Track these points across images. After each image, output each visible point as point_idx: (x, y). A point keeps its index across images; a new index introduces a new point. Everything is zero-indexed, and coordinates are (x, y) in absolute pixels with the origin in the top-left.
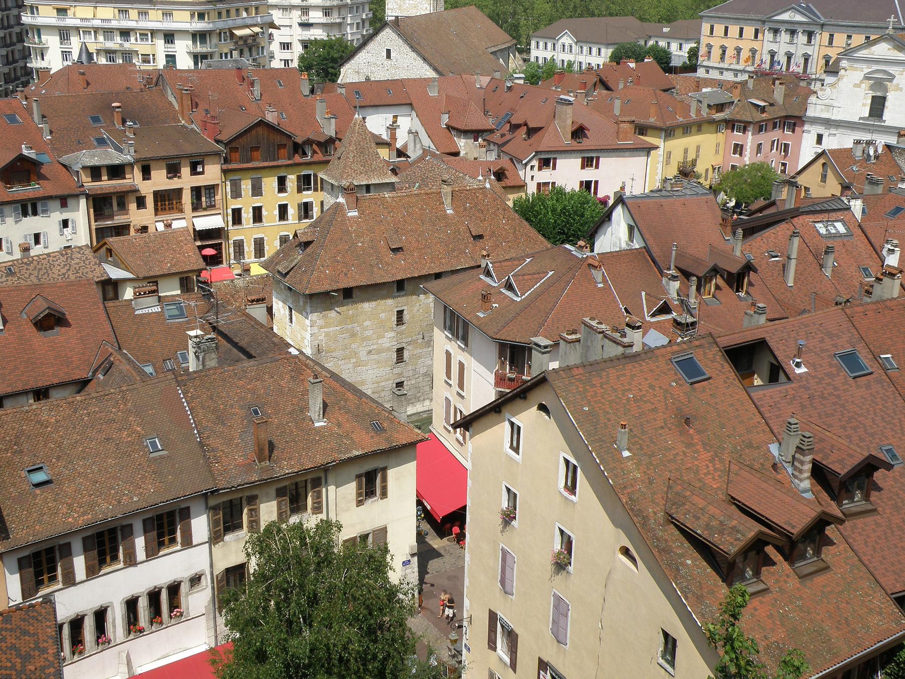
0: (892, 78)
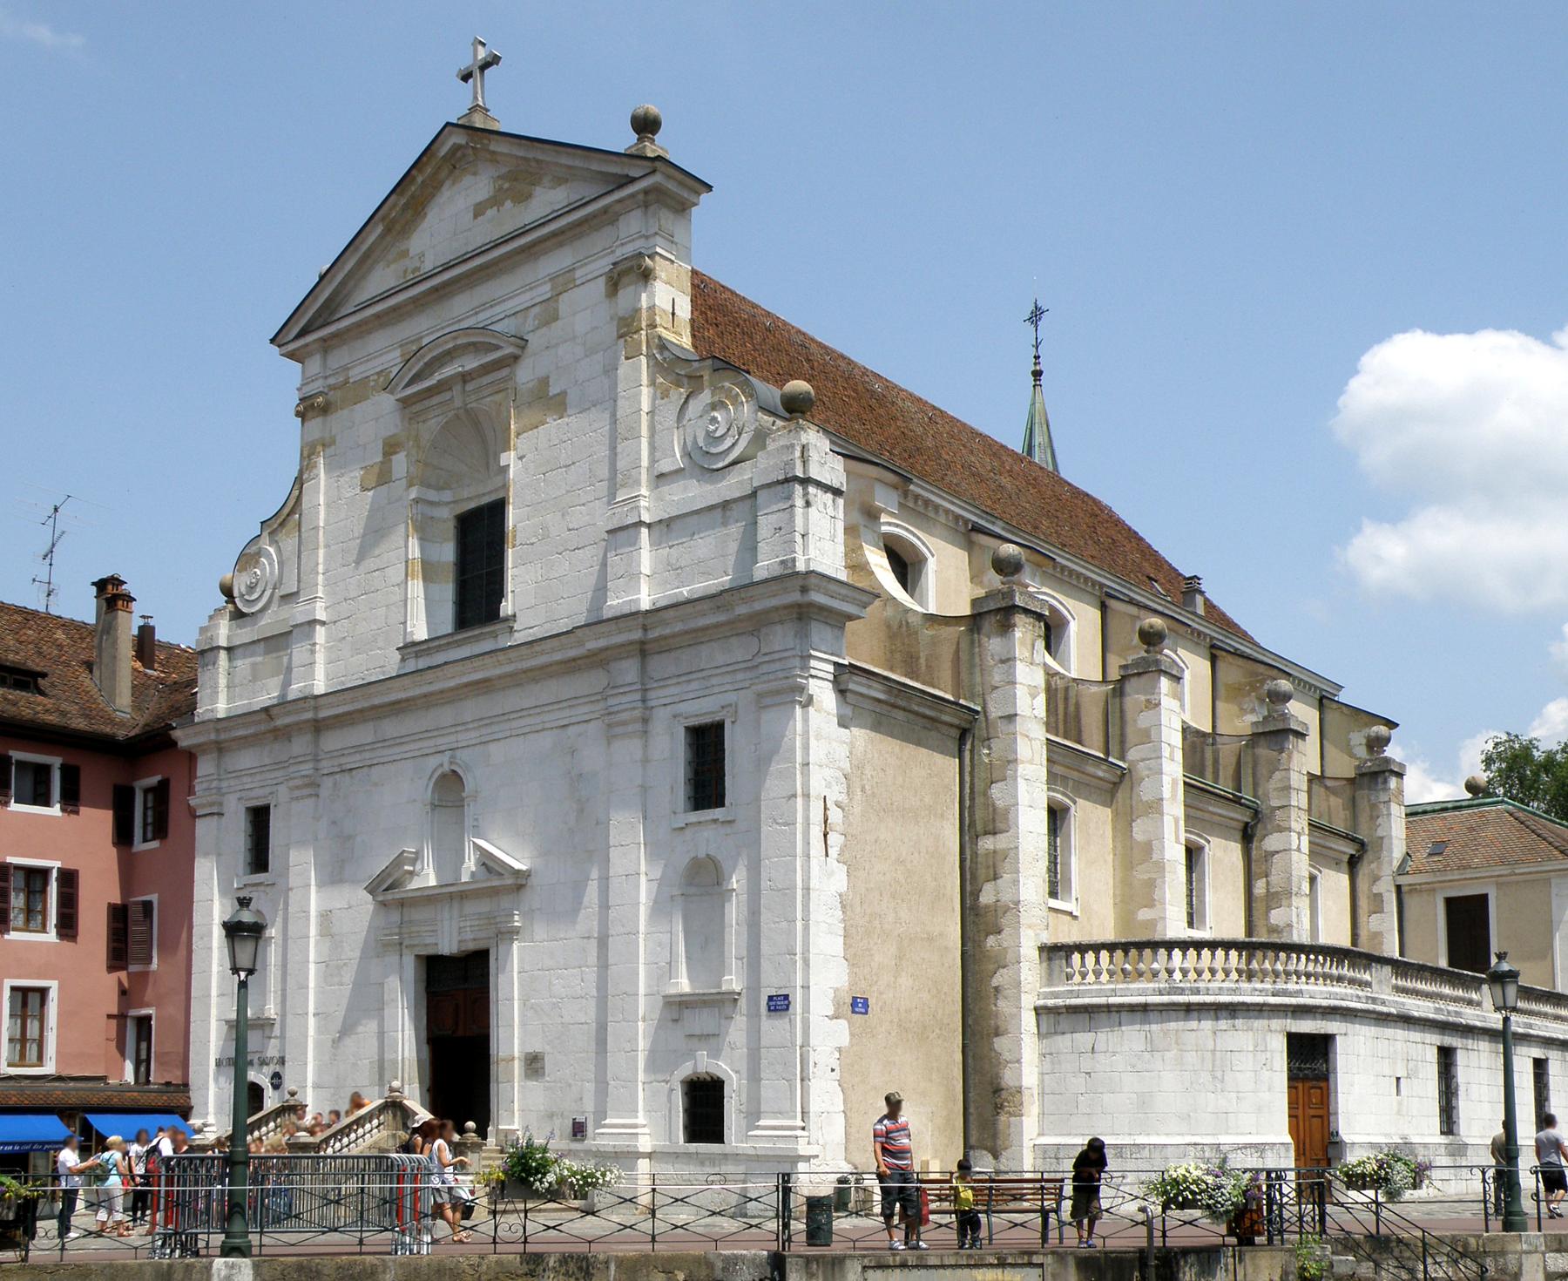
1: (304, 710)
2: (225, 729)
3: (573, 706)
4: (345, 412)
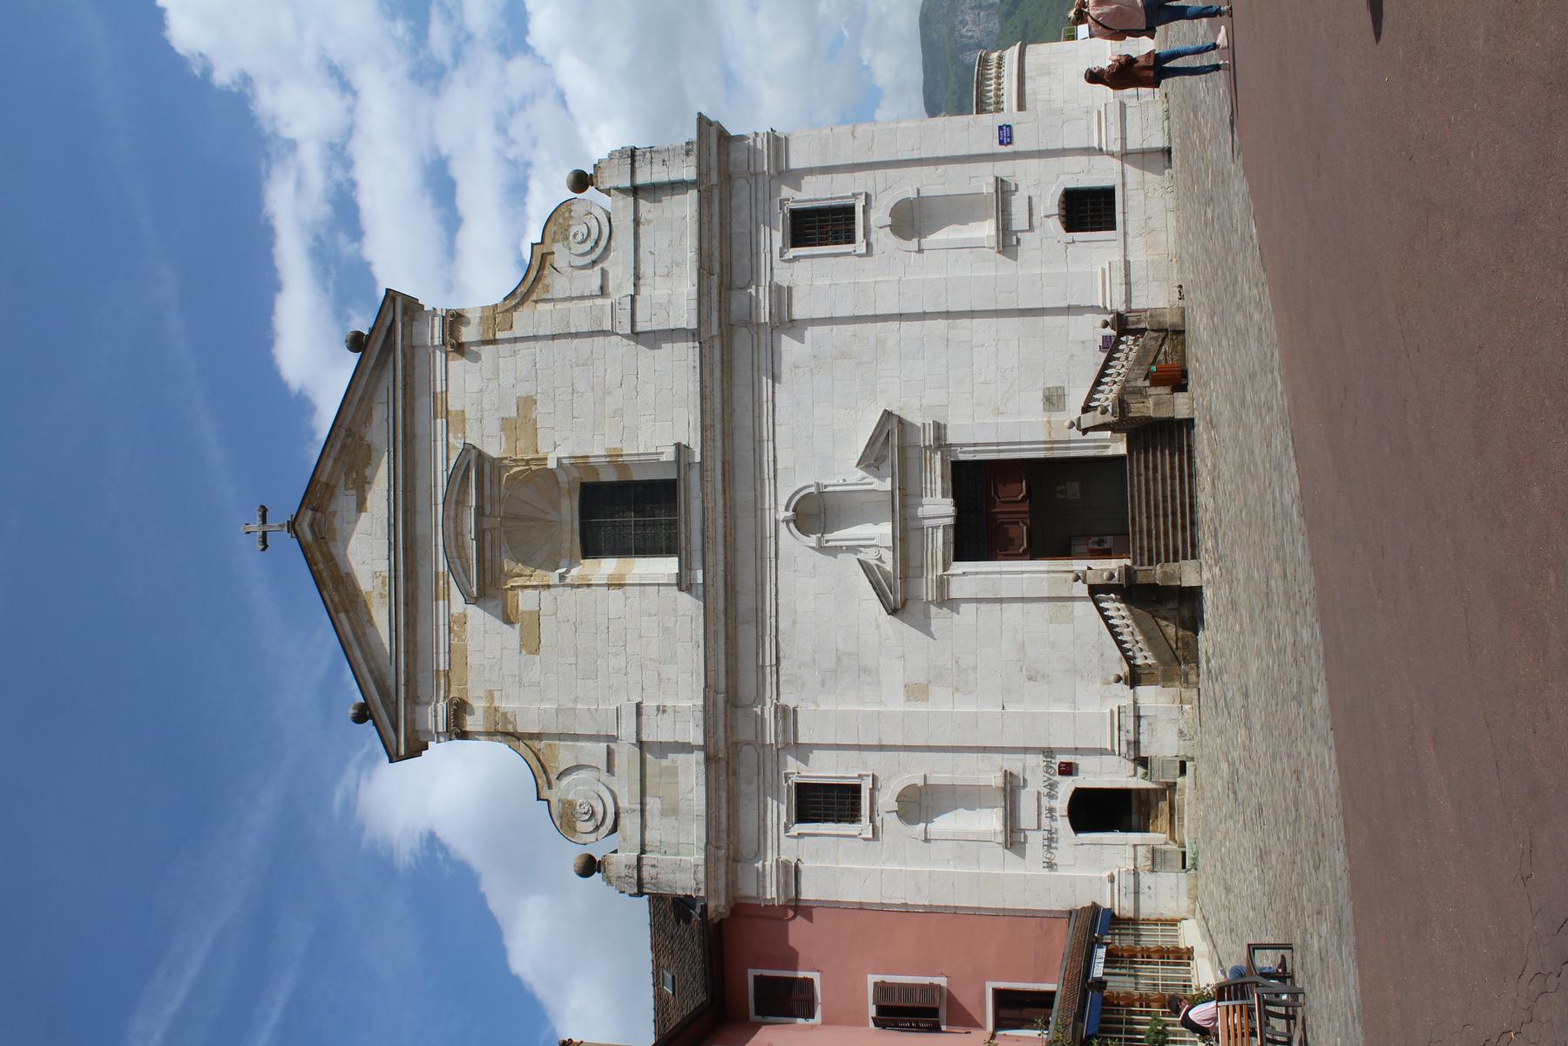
0: (475, 465)
1: (715, 704)
2: (718, 831)
4: (471, 677)
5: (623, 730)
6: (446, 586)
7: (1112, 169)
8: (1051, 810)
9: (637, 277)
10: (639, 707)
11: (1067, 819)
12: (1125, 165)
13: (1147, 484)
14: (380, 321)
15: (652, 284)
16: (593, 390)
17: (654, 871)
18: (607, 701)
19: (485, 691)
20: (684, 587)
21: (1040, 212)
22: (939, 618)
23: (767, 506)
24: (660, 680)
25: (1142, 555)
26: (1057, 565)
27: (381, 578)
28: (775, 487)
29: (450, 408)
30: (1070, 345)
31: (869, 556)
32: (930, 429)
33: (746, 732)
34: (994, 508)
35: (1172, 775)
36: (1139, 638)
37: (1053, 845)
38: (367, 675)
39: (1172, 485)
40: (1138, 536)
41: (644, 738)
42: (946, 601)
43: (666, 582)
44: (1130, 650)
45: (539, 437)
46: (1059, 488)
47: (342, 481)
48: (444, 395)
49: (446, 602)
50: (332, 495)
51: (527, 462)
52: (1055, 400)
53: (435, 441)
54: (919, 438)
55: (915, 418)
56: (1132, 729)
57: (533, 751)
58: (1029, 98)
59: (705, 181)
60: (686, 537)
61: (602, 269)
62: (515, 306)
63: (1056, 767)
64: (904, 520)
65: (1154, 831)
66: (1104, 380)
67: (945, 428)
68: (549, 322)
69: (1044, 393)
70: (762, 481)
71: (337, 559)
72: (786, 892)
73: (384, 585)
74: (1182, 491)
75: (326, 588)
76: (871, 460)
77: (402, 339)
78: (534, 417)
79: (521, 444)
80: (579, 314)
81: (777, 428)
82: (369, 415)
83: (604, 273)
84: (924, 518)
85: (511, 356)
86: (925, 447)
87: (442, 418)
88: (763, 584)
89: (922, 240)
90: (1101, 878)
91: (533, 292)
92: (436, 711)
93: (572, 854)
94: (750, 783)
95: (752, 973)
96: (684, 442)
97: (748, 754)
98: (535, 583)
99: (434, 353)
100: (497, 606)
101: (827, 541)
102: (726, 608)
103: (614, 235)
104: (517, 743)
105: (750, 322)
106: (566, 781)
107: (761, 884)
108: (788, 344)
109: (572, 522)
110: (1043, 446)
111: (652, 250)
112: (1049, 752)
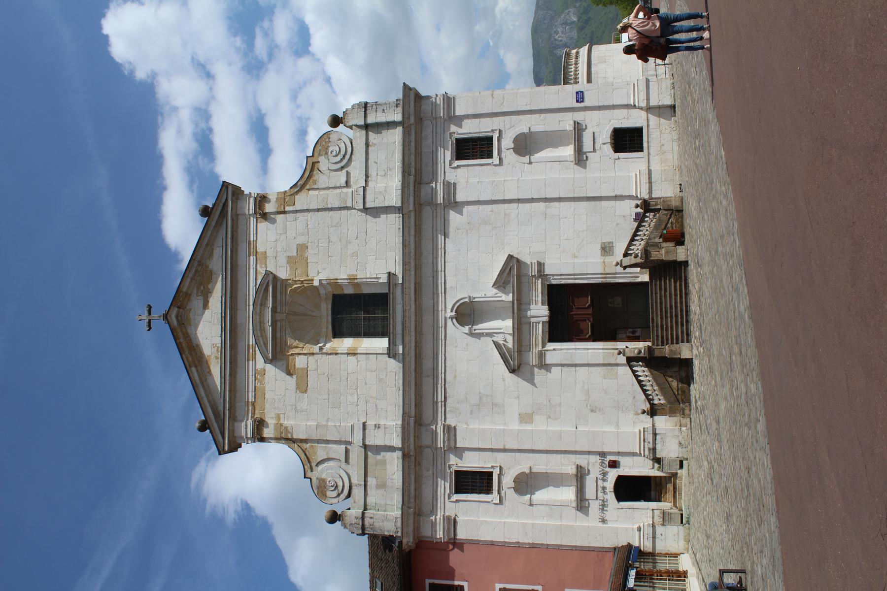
0: (272, 282)
1: (408, 424)
2: (409, 498)
3: (436, 230)
4: (267, 406)
5: (355, 438)
6: (254, 353)
7: (641, 117)
8: (604, 488)
9: (367, 176)
10: (364, 424)
11: (613, 494)
12: (649, 115)
13: (661, 299)
14: (219, 200)
15: (376, 180)
16: (340, 241)
17: (372, 520)
18: (346, 421)
19: (275, 414)
20: (391, 355)
21: (599, 141)
22: (539, 375)
23: (440, 309)
24: (377, 409)
25: (657, 339)
26: (608, 345)
27: (216, 348)
28: (445, 298)
29: (258, 250)
30: (616, 217)
31: (499, 339)
32: (535, 265)
33: (426, 440)
34: (572, 311)
35: (675, 468)
36: (656, 388)
37: (605, 509)
38: (207, 404)
39: (676, 299)
40: (655, 329)
41: (367, 443)
42: (544, 366)
43: (381, 352)
44: (650, 395)
45: (309, 268)
46: (610, 300)
47: (195, 291)
48: (255, 243)
49: (254, 362)
50: (189, 300)
51: (302, 282)
52: (607, 249)
53: (249, 269)
54: (528, 271)
55: (527, 259)
56: (651, 441)
57: (302, 449)
58: (593, 76)
59: (407, 121)
60: (393, 326)
61: (347, 171)
62: (296, 192)
63: (607, 463)
64: (519, 318)
65: (664, 501)
66: (636, 238)
67: (544, 265)
68: (316, 202)
69: (601, 245)
70: (438, 294)
71: (191, 336)
72: (448, 534)
73: (218, 352)
74: (681, 303)
75: (184, 353)
76: (501, 283)
77: (231, 210)
78: (306, 256)
79: (298, 272)
80: (333, 199)
81: (446, 264)
82: (211, 254)
83: (348, 174)
84: (531, 317)
85: (294, 221)
86: (532, 276)
87: (253, 256)
88: (437, 355)
89: (532, 157)
90: (633, 529)
91: (307, 184)
92: (246, 425)
93: (325, 510)
94: (428, 470)
95: (428, 582)
96: (393, 272)
97: (428, 453)
98: (305, 352)
99: (250, 218)
100: (283, 365)
101: (475, 330)
102: (416, 368)
103: (354, 152)
104: (293, 445)
105: (432, 203)
106: (321, 467)
107: (434, 529)
108: (453, 216)
109: (327, 316)
110: (600, 276)
111: (376, 161)
112: (603, 454)
